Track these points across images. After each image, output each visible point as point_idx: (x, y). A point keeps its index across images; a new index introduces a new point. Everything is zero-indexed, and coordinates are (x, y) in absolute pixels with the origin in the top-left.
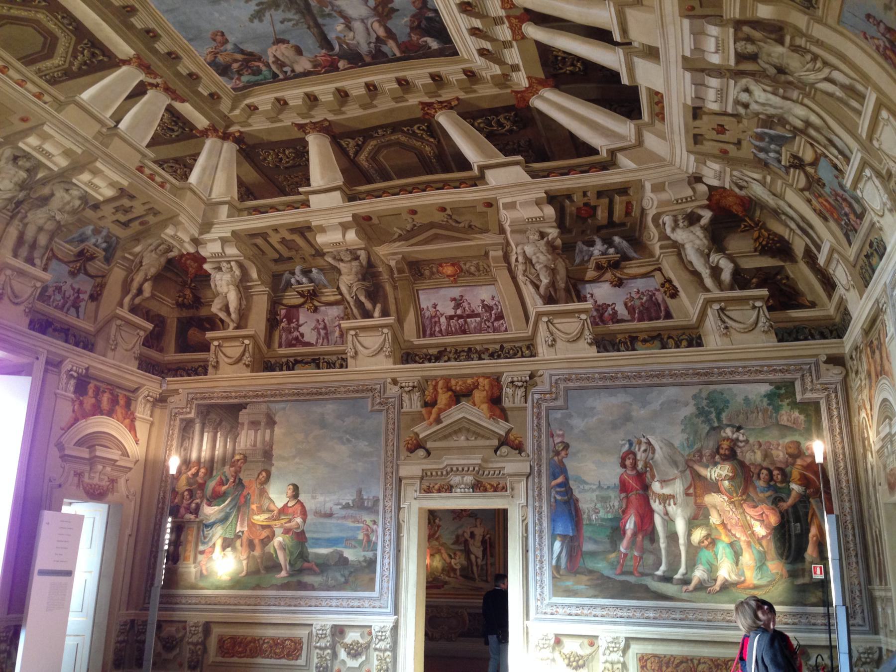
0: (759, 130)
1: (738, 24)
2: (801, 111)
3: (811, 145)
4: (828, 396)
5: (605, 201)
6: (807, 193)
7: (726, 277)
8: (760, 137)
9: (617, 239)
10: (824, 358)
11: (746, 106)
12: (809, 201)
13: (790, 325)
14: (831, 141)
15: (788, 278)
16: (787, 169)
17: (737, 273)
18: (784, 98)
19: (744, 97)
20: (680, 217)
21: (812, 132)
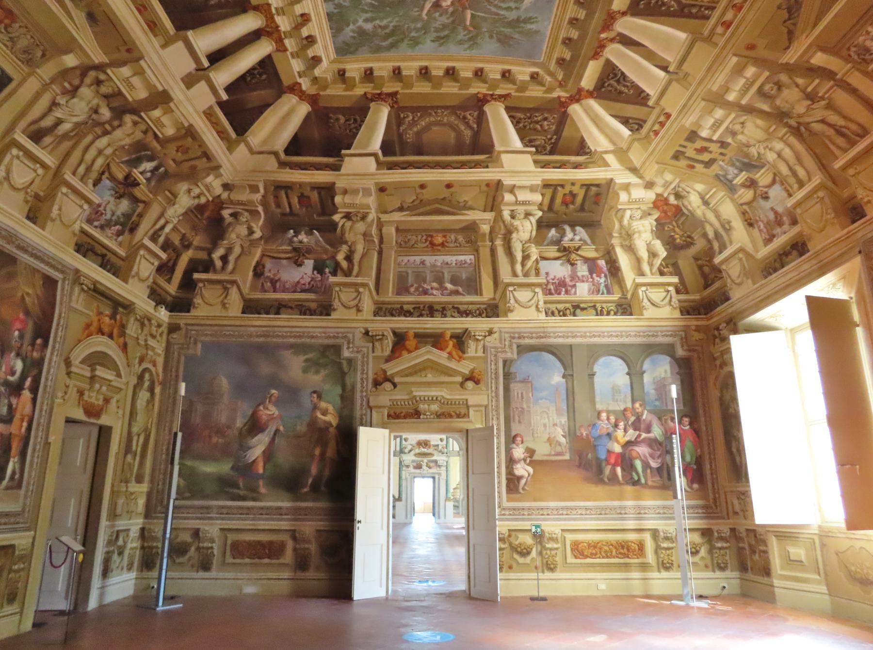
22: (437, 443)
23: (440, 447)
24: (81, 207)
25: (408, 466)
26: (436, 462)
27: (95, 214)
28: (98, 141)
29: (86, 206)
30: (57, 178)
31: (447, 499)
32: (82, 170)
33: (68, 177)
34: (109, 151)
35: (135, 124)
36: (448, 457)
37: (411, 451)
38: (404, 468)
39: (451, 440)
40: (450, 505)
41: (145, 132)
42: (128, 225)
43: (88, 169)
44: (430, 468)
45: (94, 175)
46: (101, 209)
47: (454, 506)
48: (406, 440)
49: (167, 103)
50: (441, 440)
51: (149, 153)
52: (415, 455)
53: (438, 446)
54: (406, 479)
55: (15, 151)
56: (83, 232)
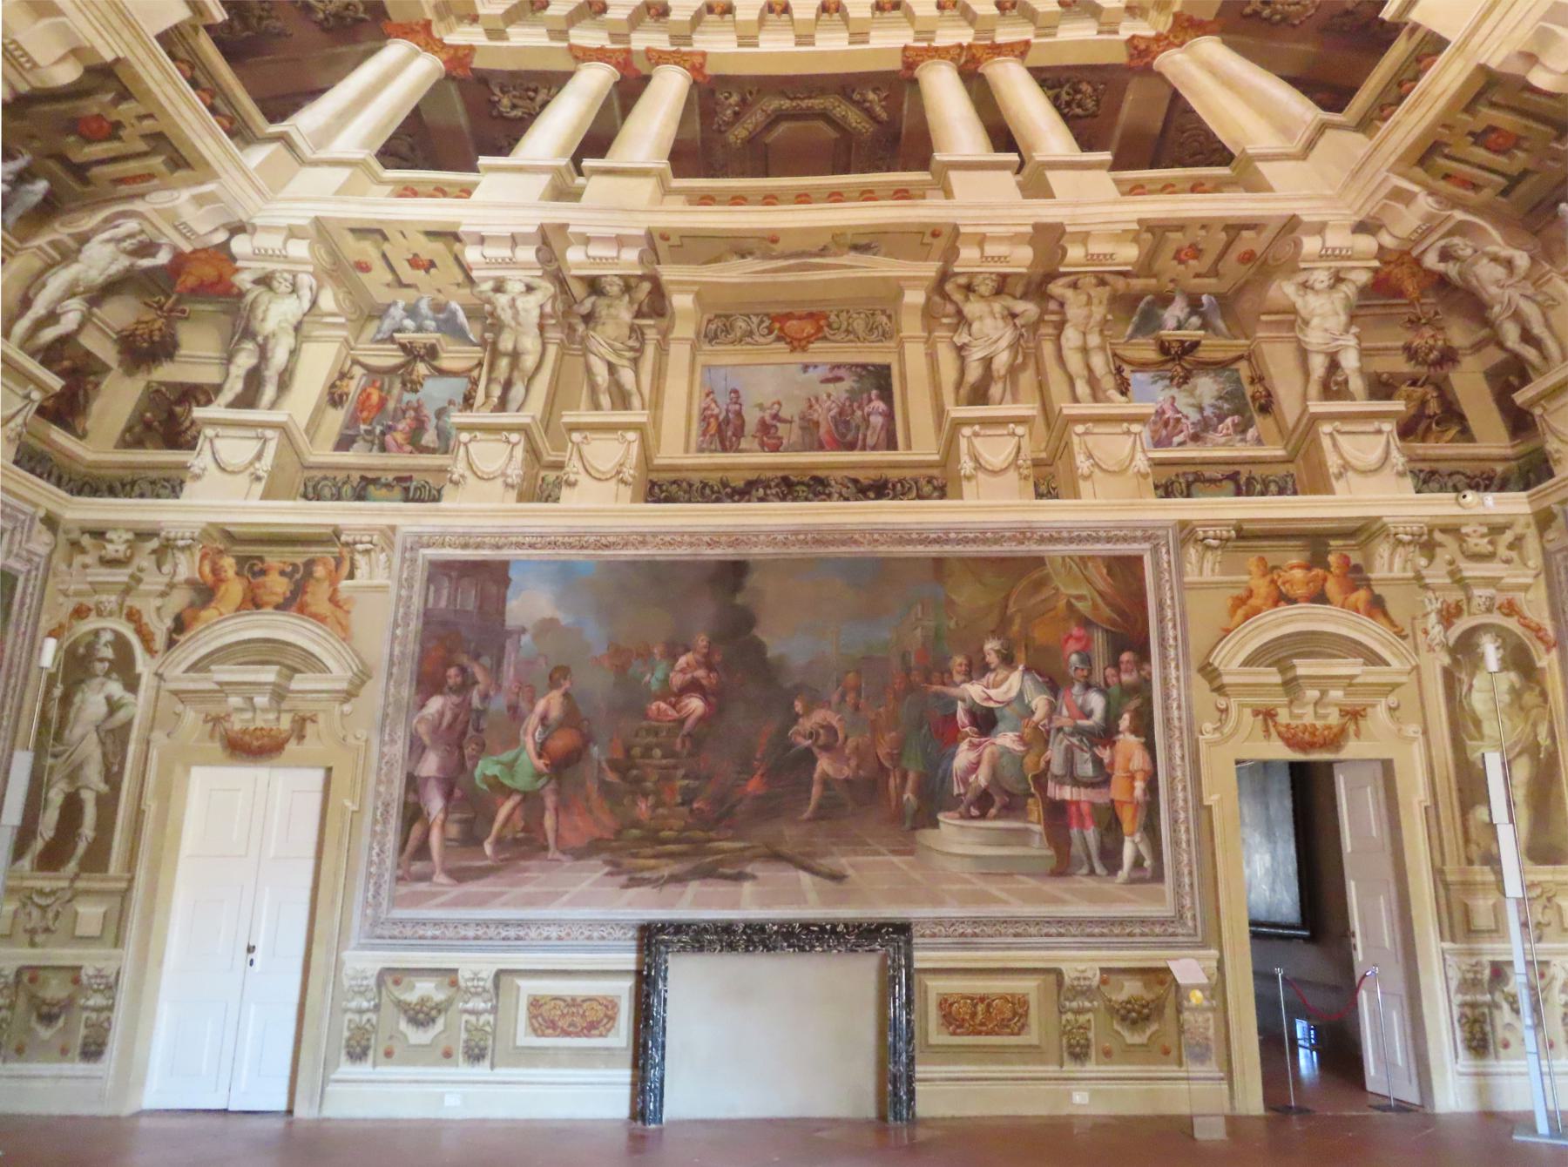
0: (454, 305)
1: (655, 281)
2: (530, 343)
3: (480, 364)
4: (29, 572)
5: (142, 146)
6: (358, 371)
7: (49, 334)
8: (438, 308)
9: (41, 186)
10: (41, 513)
11: (499, 288)
12: (343, 376)
13: (39, 446)
14: (508, 385)
15: (97, 385)
16: (392, 340)
17: (65, 340)
18: (542, 328)
19: (515, 287)
20: (142, 237)
21: (504, 363)
24: (1128, 433)
27: (1164, 428)
28: (1063, 341)
29: (1136, 428)
30: (1056, 426)
32: (1082, 388)
33: (1070, 409)
34: (1094, 340)
35: (1074, 286)
41: (1102, 282)
42: (1251, 403)
43: (1093, 381)
45: (1108, 382)
46: (1169, 414)
49: (1064, 232)
51: (1149, 298)
55: (967, 431)
56: (1158, 464)
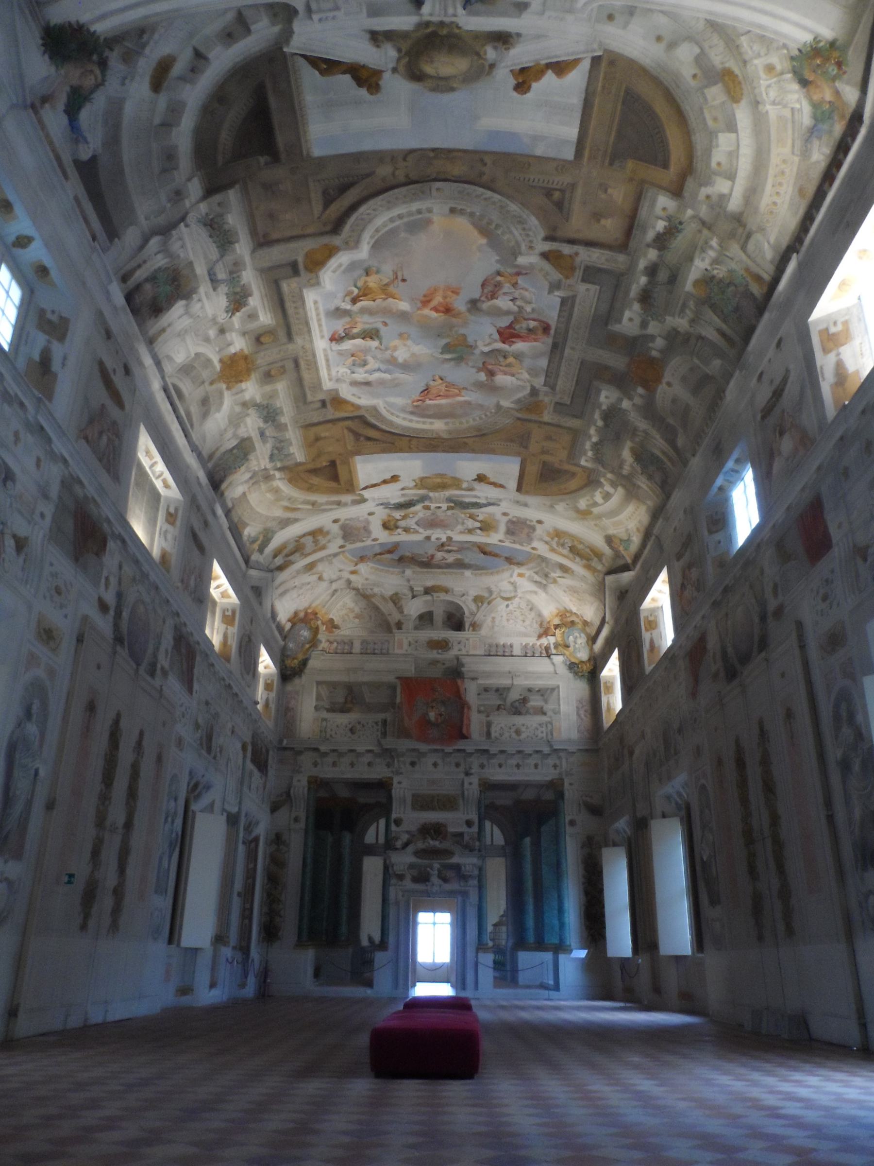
22: (460, 830)
23: (466, 838)
25: (401, 877)
26: (457, 868)
31: (481, 947)
36: (483, 858)
37: (406, 845)
38: (394, 881)
39: (488, 824)
40: (487, 959)
44: (445, 880)
47: (495, 962)
48: (398, 822)
50: (469, 823)
52: (418, 853)
53: (461, 835)
54: (397, 903)
